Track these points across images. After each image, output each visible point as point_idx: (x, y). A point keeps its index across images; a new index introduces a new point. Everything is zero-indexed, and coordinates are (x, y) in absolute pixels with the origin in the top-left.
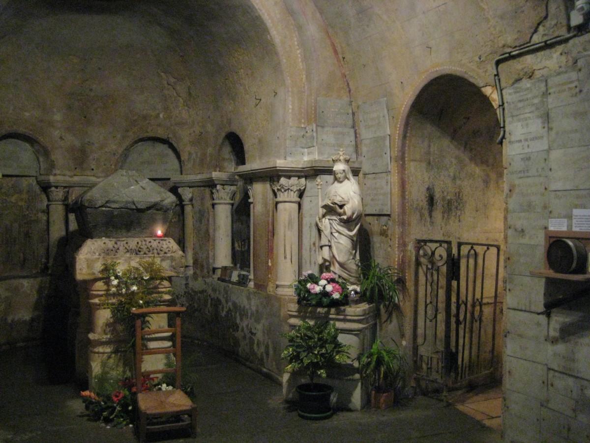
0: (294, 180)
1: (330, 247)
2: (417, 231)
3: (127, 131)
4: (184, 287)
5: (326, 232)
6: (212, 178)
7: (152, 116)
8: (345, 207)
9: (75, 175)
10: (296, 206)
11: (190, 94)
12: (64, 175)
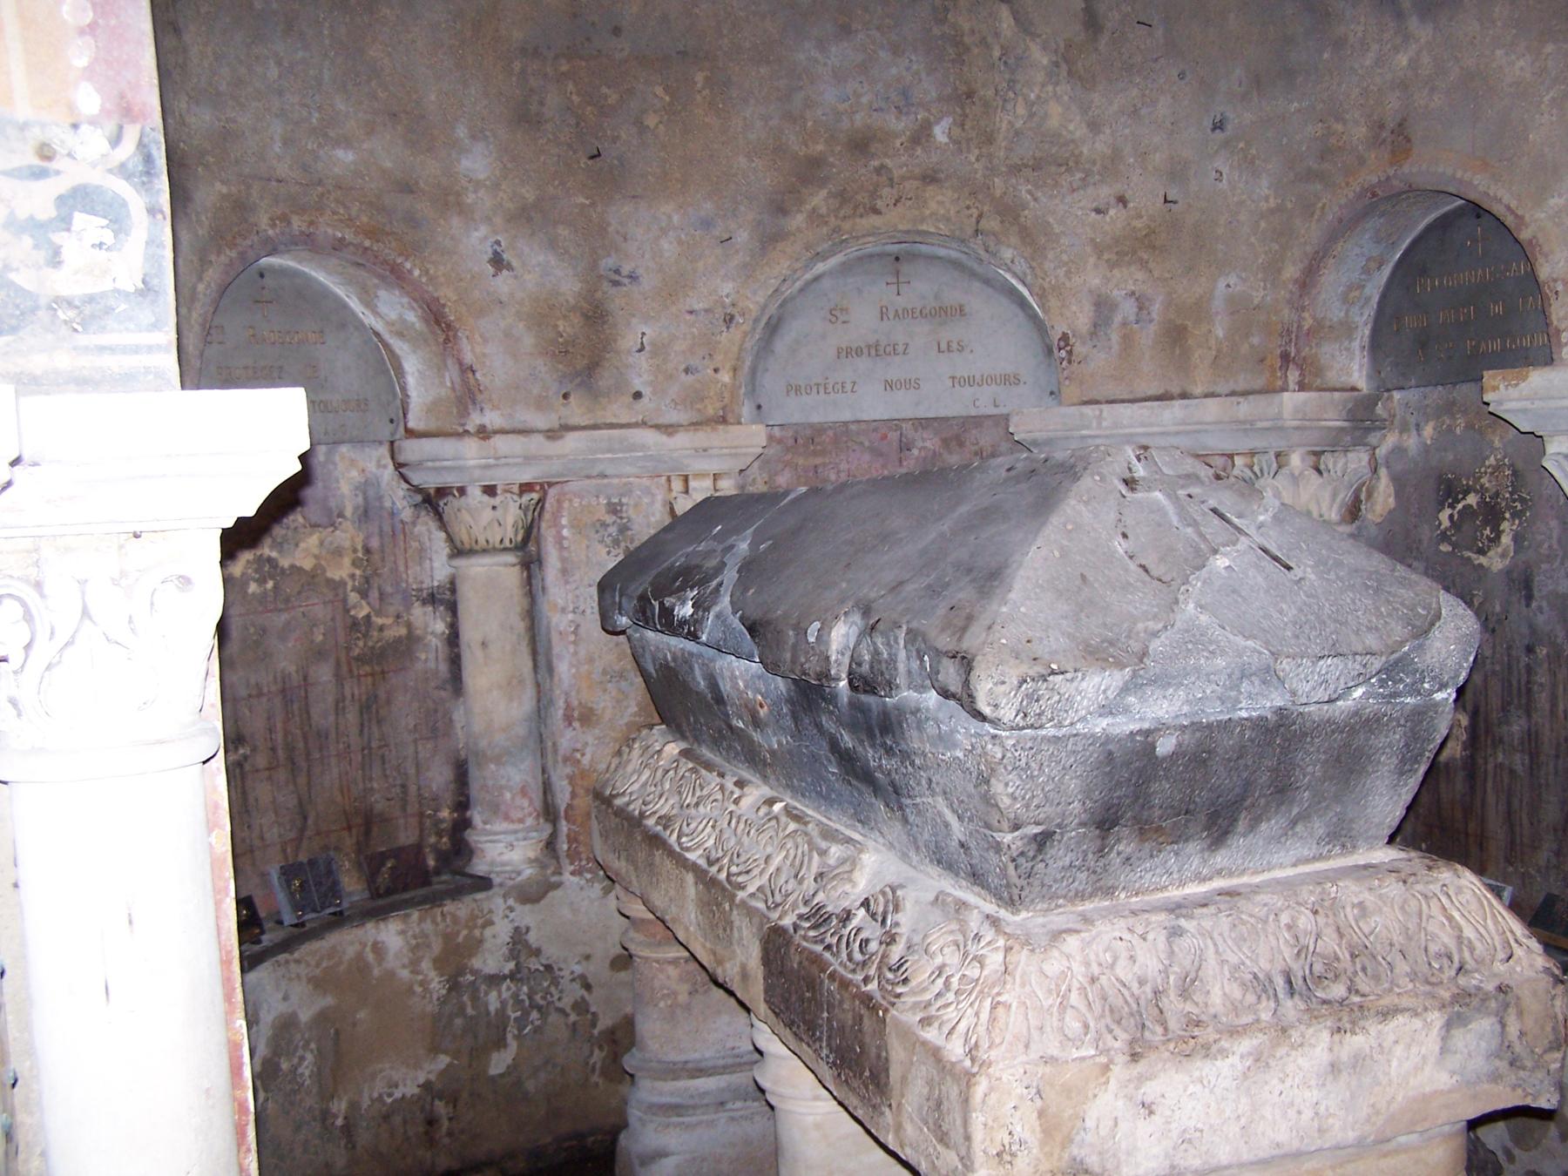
3: (781, 210)
9: (567, 428)
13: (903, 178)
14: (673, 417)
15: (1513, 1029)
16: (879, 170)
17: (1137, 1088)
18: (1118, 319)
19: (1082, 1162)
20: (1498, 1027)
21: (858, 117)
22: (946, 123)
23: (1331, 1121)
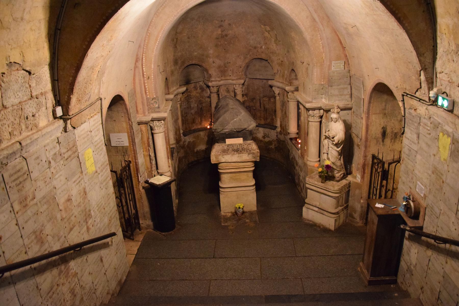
0: (316, 112)
1: (327, 154)
2: (373, 150)
3: (247, 55)
4: (275, 136)
5: (326, 147)
8: (335, 138)
9: (222, 80)
10: (319, 123)
12: (216, 81)
14: (234, 78)
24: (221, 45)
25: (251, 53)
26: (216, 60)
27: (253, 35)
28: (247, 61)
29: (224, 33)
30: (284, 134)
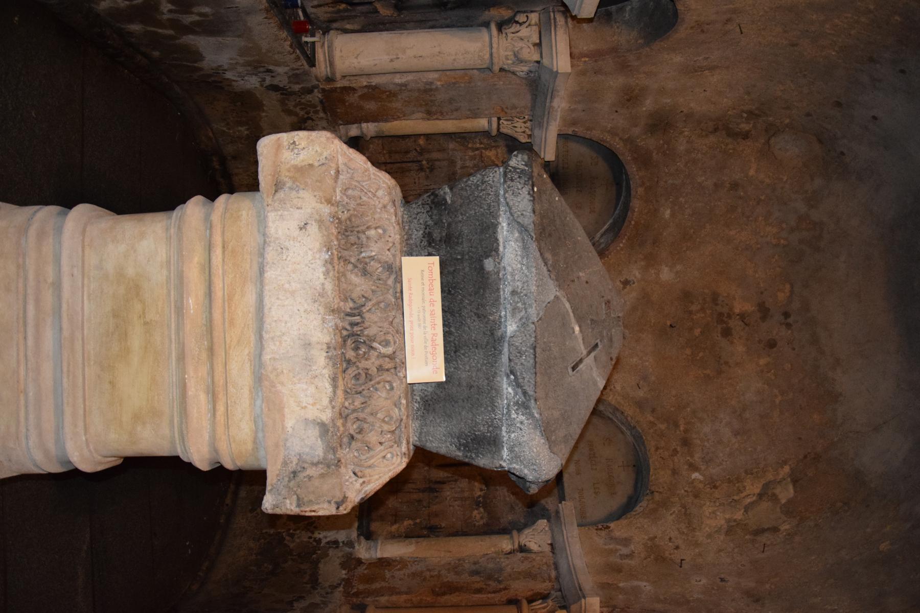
3: (653, 411)
6: (584, 597)
7: (692, 456)
11: (760, 532)
13: (673, 461)
15: (312, 471)
16: (675, 450)
17: (316, 220)
18: (619, 547)
19: (281, 188)
20: (315, 460)
21: (699, 442)
22: (701, 478)
23: (278, 343)
24: (691, 313)
25: (663, 427)
26: (634, 294)
27: (736, 433)
28: (629, 411)
29: (735, 324)
30: (348, 582)
